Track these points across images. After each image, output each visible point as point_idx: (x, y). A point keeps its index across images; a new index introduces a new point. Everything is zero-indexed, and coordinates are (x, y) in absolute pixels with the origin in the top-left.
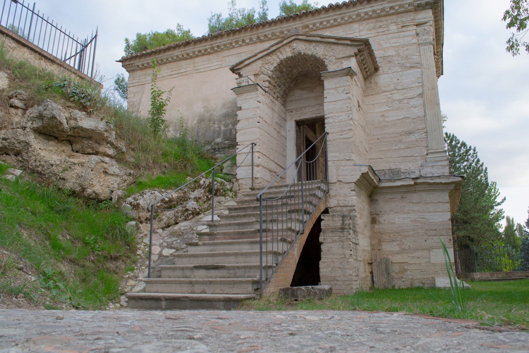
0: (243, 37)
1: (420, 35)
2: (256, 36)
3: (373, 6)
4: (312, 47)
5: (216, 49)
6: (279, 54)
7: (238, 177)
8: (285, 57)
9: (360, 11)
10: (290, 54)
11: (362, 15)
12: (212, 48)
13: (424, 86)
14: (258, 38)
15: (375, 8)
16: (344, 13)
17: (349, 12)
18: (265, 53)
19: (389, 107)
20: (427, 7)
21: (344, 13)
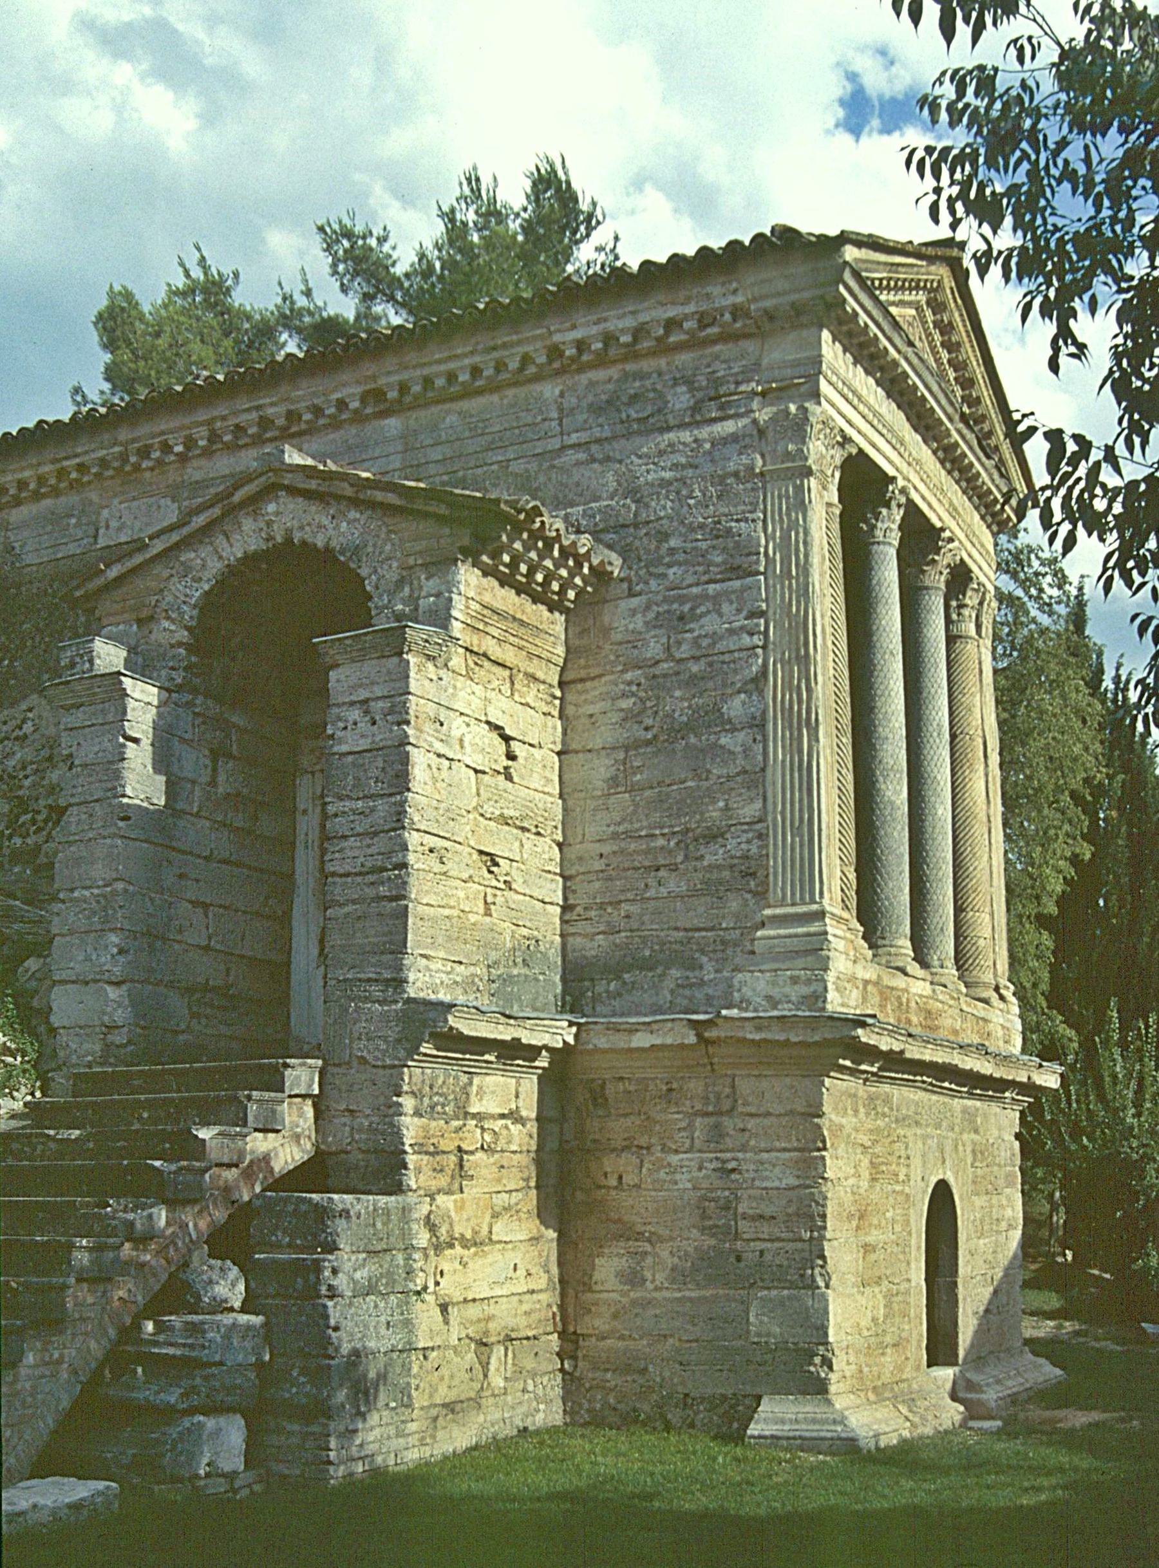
0: (163, 433)
1: (770, 434)
2: (204, 431)
3: (606, 320)
4: (326, 521)
5: (74, 475)
6: (220, 540)
7: (55, 1021)
8: (239, 555)
9: (557, 338)
10: (255, 544)
11: (568, 353)
12: (61, 474)
13: (771, 647)
14: (214, 437)
15: (610, 326)
16: (505, 346)
17: (519, 343)
18: (175, 537)
19: (647, 729)
20: (804, 319)
21: (505, 346)
